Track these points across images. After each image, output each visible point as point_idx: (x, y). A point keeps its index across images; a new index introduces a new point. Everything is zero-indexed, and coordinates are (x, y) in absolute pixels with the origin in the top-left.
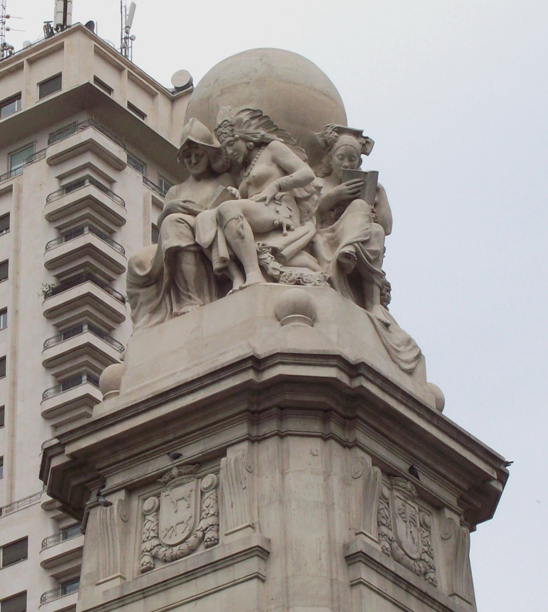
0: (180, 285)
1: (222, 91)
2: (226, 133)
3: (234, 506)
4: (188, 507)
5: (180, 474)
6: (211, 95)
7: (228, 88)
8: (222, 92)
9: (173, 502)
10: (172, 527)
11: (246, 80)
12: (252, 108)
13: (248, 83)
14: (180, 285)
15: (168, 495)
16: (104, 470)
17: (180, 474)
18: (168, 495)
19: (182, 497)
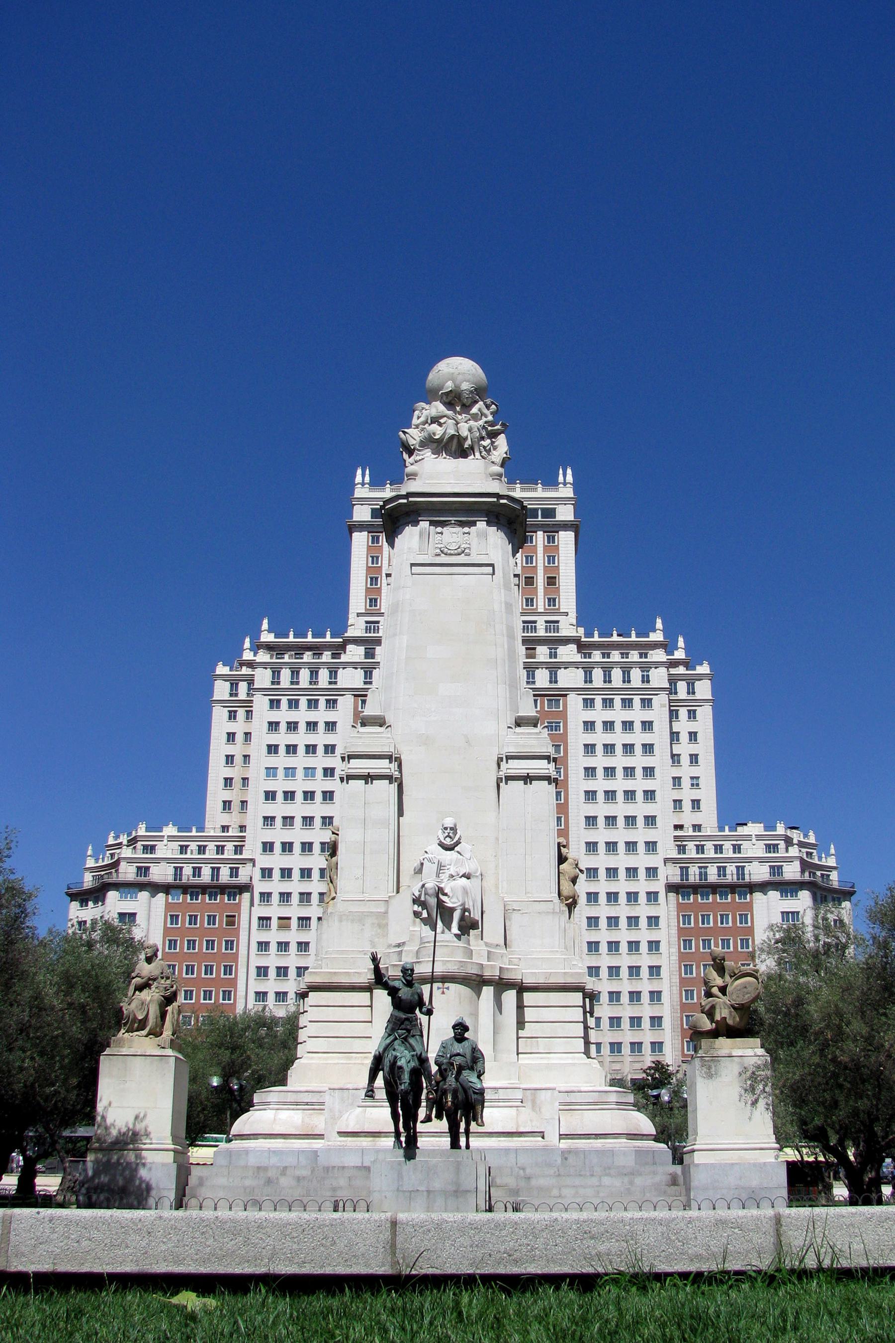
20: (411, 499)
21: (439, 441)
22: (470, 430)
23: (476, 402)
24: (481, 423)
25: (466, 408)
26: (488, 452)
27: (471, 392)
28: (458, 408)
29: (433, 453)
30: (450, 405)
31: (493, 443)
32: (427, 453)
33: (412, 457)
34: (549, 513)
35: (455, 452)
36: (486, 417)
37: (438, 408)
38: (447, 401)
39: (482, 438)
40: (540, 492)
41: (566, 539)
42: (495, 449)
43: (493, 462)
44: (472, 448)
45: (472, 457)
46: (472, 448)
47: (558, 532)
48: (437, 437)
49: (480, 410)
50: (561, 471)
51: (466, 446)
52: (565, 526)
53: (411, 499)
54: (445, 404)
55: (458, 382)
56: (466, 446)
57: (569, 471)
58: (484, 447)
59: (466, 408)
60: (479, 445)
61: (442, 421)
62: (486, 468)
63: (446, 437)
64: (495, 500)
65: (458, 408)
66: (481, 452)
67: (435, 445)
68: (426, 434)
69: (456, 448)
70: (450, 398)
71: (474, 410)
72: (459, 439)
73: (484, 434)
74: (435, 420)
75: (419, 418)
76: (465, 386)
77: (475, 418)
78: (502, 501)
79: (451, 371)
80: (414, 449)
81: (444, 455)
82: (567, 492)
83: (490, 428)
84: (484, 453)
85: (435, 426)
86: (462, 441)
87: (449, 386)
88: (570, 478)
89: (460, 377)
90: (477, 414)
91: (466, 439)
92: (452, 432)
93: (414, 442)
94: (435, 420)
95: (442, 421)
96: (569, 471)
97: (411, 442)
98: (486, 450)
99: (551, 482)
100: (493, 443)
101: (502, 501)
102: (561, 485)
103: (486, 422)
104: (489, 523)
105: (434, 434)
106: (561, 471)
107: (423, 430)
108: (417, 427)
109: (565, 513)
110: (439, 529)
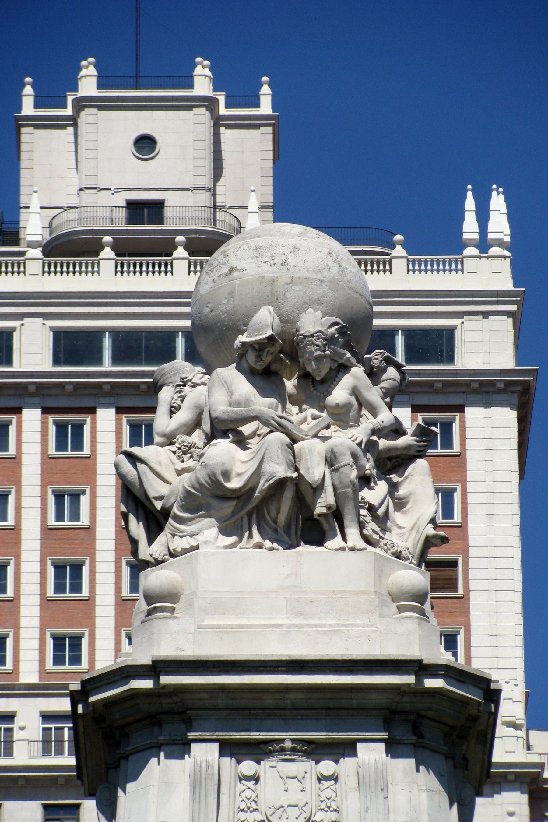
0: (269, 513)
1: (292, 279)
2: (318, 346)
3: (369, 811)
4: (302, 791)
5: (293, 750)
6: (277, 277)
7: (299, 278)
8: (292, 280)
9: (282, 778)
10: (282, 807)
11: (319, 276)
12: (342, 322)
13: (322, 282)
14: (269, 513)
15: (275, 767)
16: (194, 712)
17: (293, 750)
18: (275, 767)
19: (294, 775)
20: (165, 680)
21: (243, 495)
22: (331, 461)
23: (343, 368)
24: (360, 433)
25: (314, 387)
26: (383, 521)
27: (330, 340)
28: (290, 385)
29: (225, 531)
30: (266, 377)
31: (393, 487)
32: (207, 532)
33: (161, 539)
34: (434, 345)
35: (287, 528)
36: (374, 412)
37: (230, 388)
38: (259, 366)
39: (365, 481)
40: (400, 276)
41: (489, 435)
42: (400, 505)
43: (398, 555)
44: (337, 515)
45: (337, 542)
46: (337, 515)
47: (460, 409)
48: (234, 484)
49: (355, 392)
50: (470, 203)
51: (320, 509)
52: (486, 389)
53: (165, 680)
54: (251, 374)
55: (287, 308)
56: (320, 509)
57: (498, 202)
58: (371, 509)
59: (314, 387)
60: (358, 504)
61: (246, 429)
62: (380, 574)
63: (263, 485)
64: (410, 679)
65: (290, 385)
66: (361, 526)
67: (229, 507)
68: (202, 475)
69: (292, 515)
70: (268, 359)
71: (339, 394)
72: (301, 491)
73: (369, 466)
74: (224, 428)
75: (173, 410)
76: (313, 323)
77: (342, 417)
78: (431, 683)
79: (267, 271)
80: (166, 513)
81: (257, 537)
82: (493, 273)
83: (383, 443)
84: (371, 527)
85: (223, 447)
86: (308, 497)
87: (264, 322)
88: (499, 225)
89: (296, 294)
90: (348, 406)
91: (318, 489)
92: (278, 469)
93: (162, 489)
94: (224, 428)
95: (246, 429)
96: (498, 202)
97: (155, 488)
98: (375, 518)
99: (439, 241)
100: (393, 487)
101: (431, 683)
102: (471, 251)
103: (374, 432)
104: (393, 748)
105: (227, 475)
106: (470, 203)
107: (186, 450)
108: (169, 440)
109: (486, 346)
110: (248, 767)
